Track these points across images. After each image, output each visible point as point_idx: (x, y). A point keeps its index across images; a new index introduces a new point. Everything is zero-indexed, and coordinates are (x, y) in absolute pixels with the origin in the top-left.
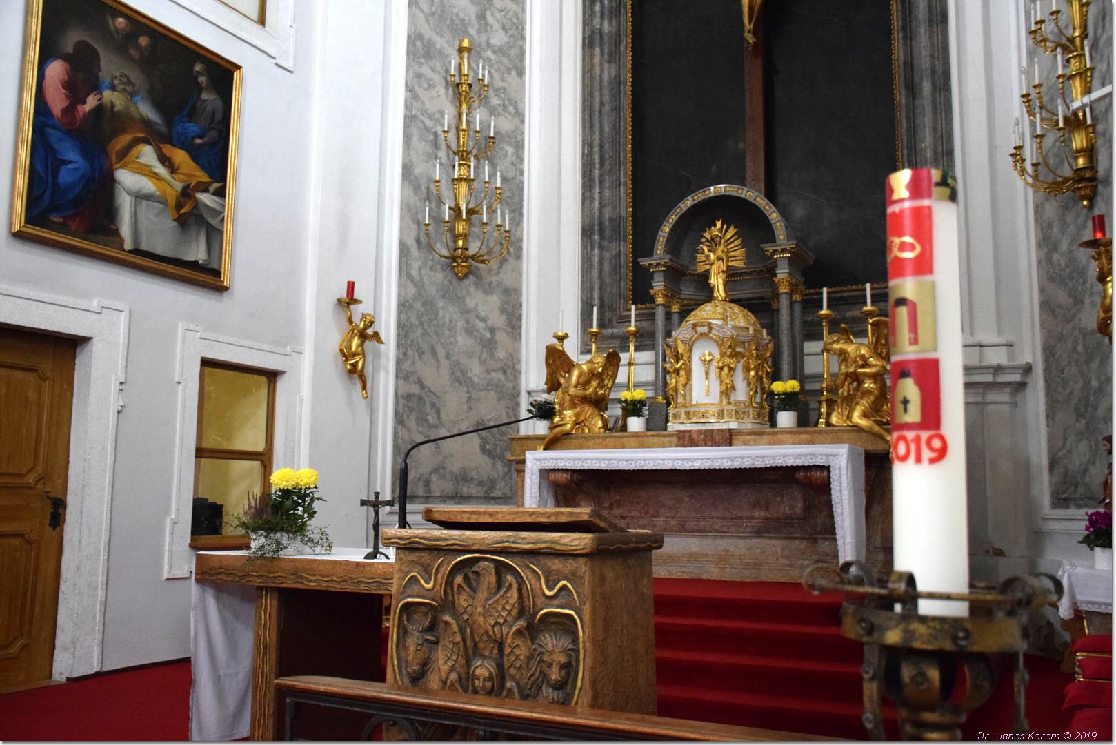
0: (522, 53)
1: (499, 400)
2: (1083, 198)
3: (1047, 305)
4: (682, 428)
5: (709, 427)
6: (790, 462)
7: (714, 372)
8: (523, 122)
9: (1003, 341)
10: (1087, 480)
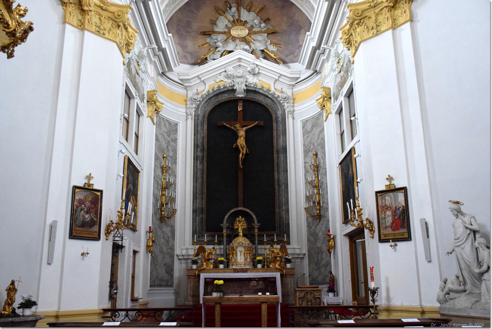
0: (176, 158)
1: (170, 257)
2: (318, 219)
3: (308, 240)
4: (235, 268)
5: (242, 268)
6: (267, 276)
7: (242, 254)
8: (176, 178)
9: (299, 248)
10: (318, 279)
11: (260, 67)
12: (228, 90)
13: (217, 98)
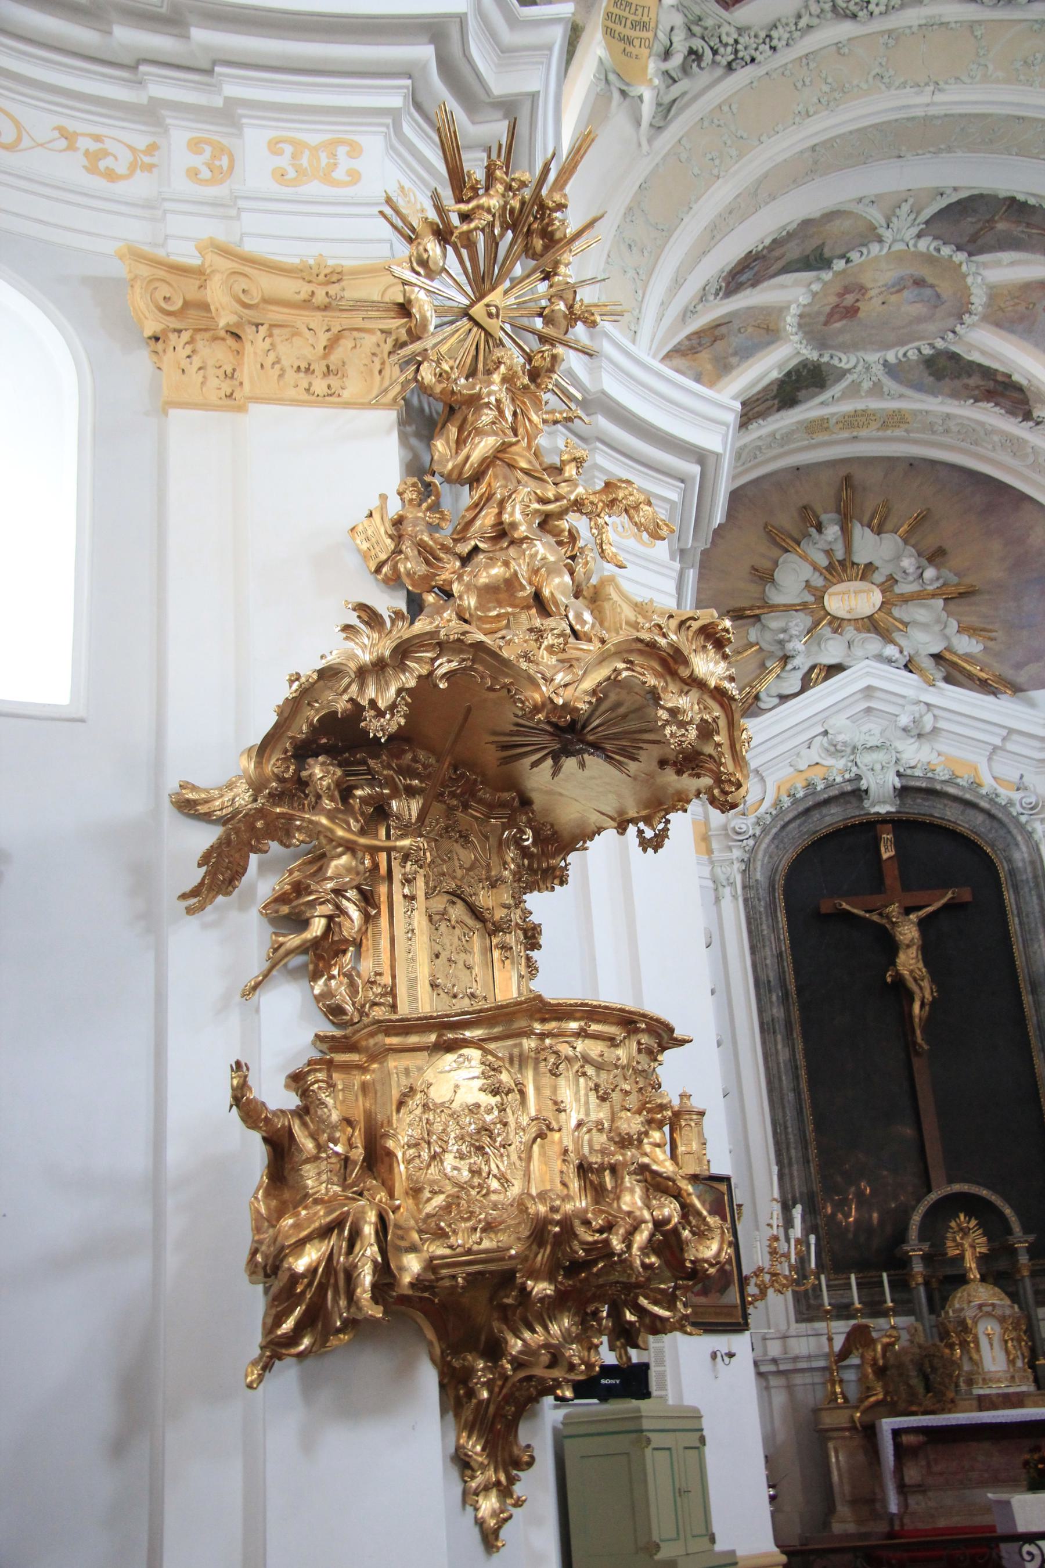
11: (937, 712)
12: (843, 795)
13: (805, 821)
